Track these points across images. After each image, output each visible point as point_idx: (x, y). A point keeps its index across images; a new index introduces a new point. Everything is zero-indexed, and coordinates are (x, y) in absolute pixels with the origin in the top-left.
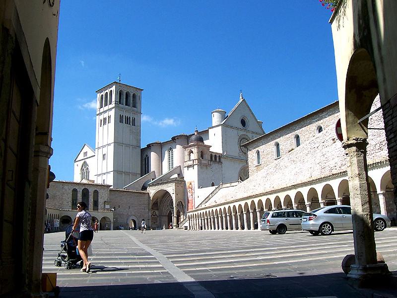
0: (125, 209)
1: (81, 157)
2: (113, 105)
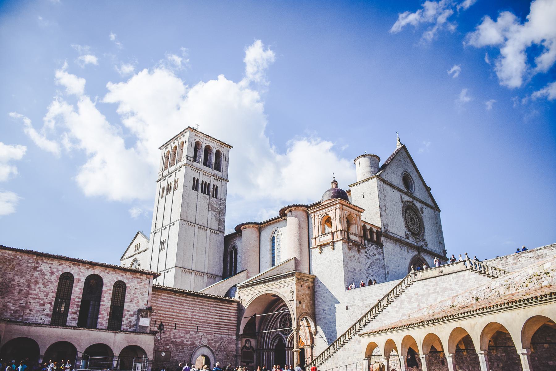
0: (188, 333)
1: (132, 251)
2: (184, 161)
